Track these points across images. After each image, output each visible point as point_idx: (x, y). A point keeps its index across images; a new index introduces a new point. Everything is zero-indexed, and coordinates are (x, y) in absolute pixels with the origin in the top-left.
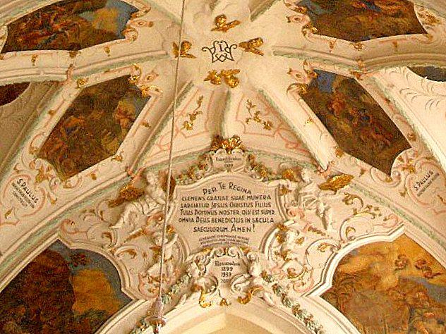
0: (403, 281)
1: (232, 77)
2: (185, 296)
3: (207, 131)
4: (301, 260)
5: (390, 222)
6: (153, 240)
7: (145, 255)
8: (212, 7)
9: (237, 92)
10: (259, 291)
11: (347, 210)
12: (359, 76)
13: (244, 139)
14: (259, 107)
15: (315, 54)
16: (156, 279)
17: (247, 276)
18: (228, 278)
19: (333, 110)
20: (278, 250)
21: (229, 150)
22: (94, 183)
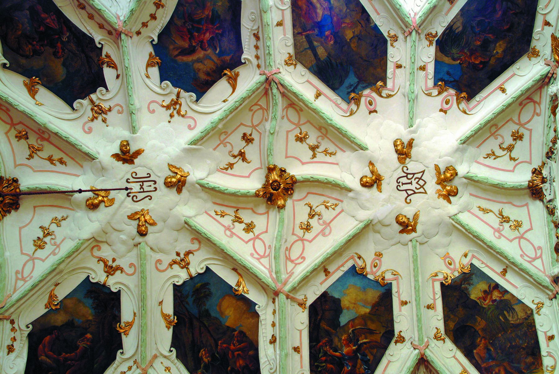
3: (527, 205)
14: (492, 144)
21: (543, 181)
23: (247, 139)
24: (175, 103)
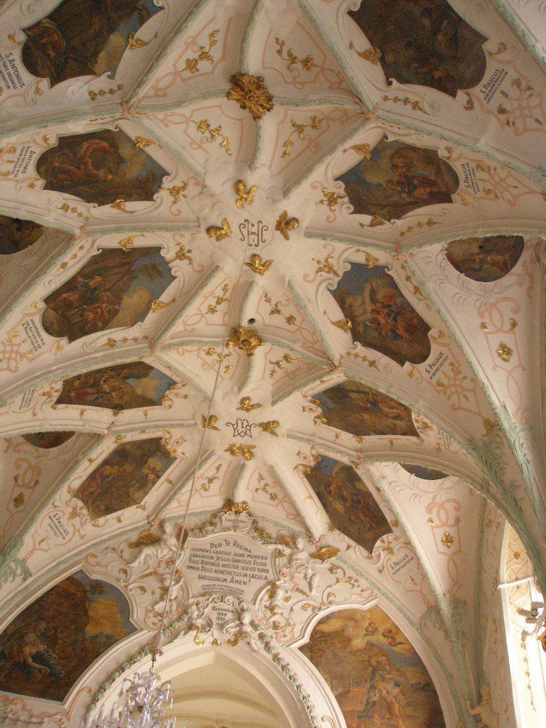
0: (371, 645)
1: (249, 451)
2: (183, 632)
4: (286, 615)
5: (366, 594)
6: (162, 580)
7: (153, 593)
8: (240, 389)
9: (251, 465)
10: (246, 637)
11: (332, 578)
12: (357, 465)
13: (252, 505)
14: (268, 480)
15: (322, 442)
16: (161, 615)
17: (237, 622)
18: (222, 622)
19: (331, 491)
20: (267, 604)
21: (237, 512)
22: (119, 525)
23: (290, 320)
24: (330, 269)
